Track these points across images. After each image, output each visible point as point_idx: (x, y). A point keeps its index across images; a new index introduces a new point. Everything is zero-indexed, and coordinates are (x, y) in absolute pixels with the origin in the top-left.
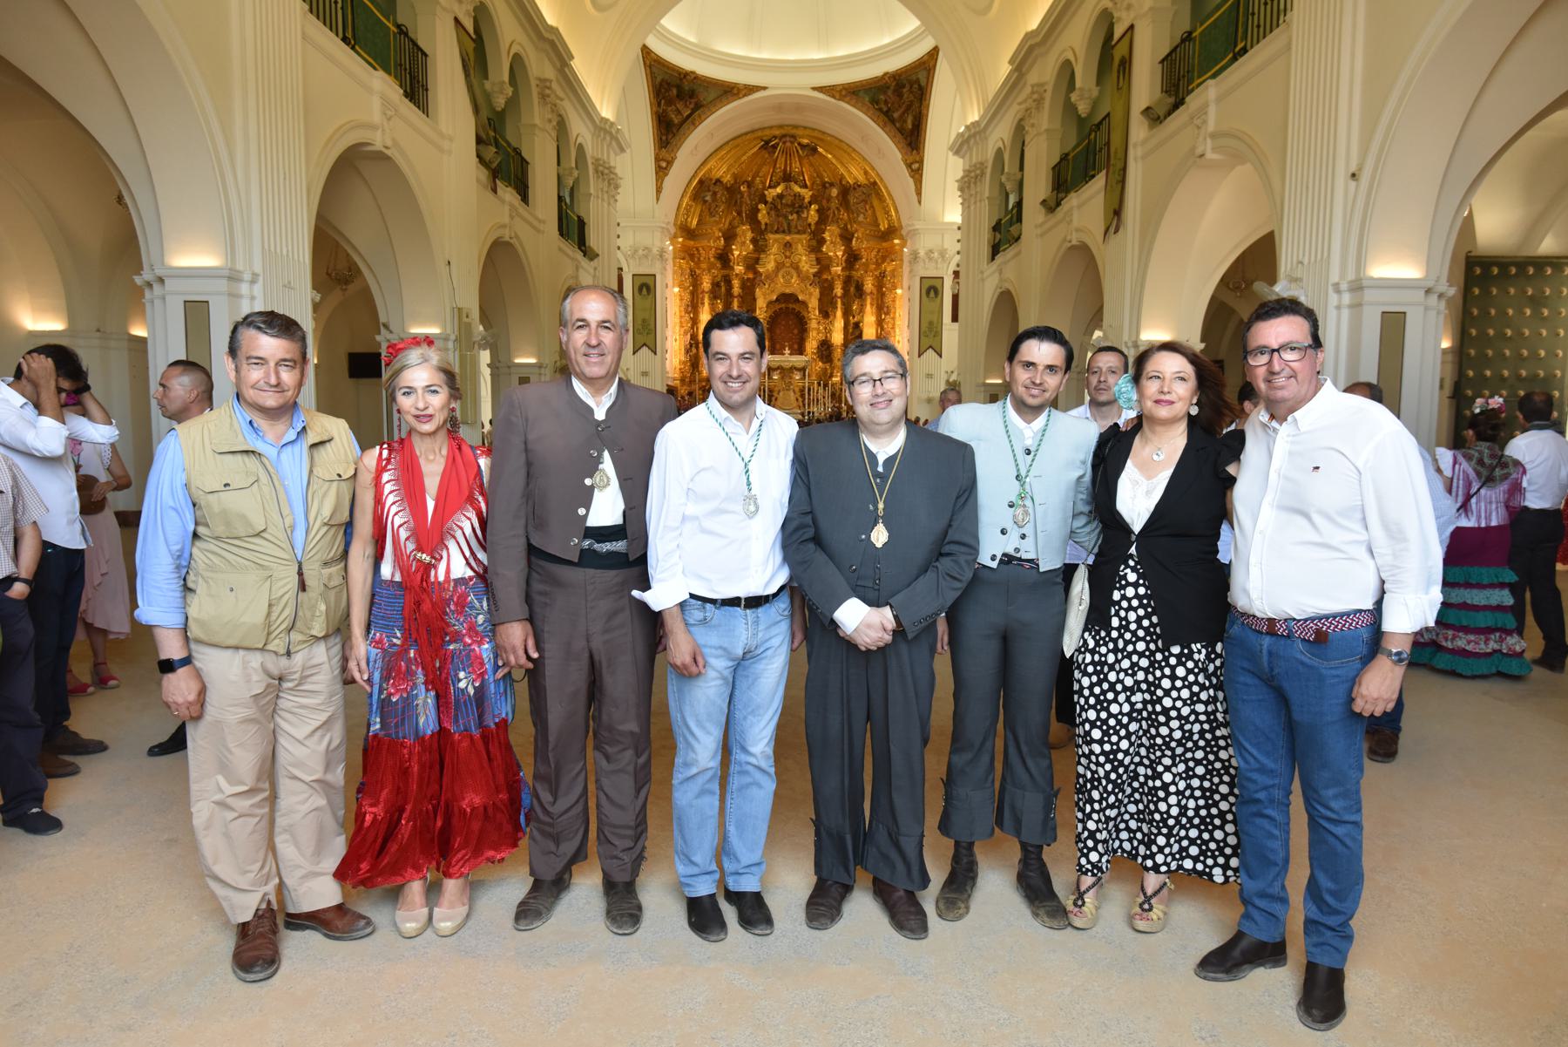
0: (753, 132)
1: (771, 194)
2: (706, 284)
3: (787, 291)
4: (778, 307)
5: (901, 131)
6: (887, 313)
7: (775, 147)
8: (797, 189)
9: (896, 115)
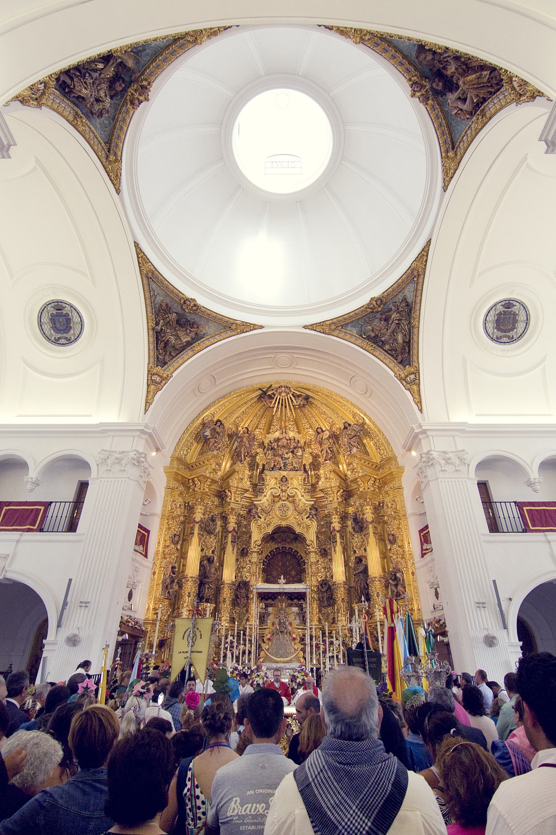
3: (284, 524)
4: (273, 546)
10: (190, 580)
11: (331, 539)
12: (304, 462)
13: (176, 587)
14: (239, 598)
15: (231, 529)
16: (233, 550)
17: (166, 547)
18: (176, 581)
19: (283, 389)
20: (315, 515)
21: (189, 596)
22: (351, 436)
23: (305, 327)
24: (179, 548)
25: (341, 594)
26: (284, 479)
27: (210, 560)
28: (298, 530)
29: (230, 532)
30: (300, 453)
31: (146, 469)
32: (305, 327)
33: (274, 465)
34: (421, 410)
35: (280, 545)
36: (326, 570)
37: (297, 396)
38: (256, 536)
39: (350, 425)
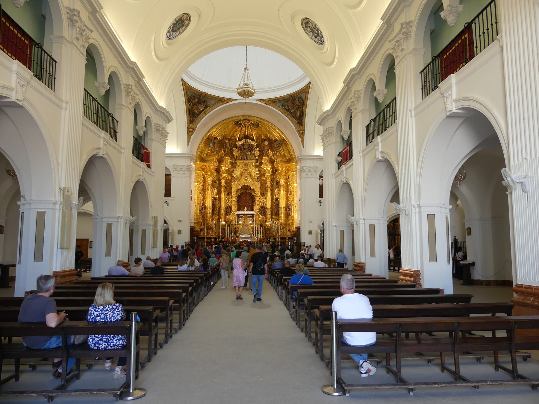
0: (231, 118)
1: (239, 143)
4: (241, 191)
5: (295, 117)
6: (290, 194)
7: (240, 124)
8: (250, 141)
9: (292, 111)
11: (266, 190)
15: (223, 186)
23: (257, 100)
25: (269, 212)
27: (215, 199)
30: (253, 153)
31: (133, 96)
32: (257, 100)
34: (303, 147)
37: (252, 124)
38: (234, 190)
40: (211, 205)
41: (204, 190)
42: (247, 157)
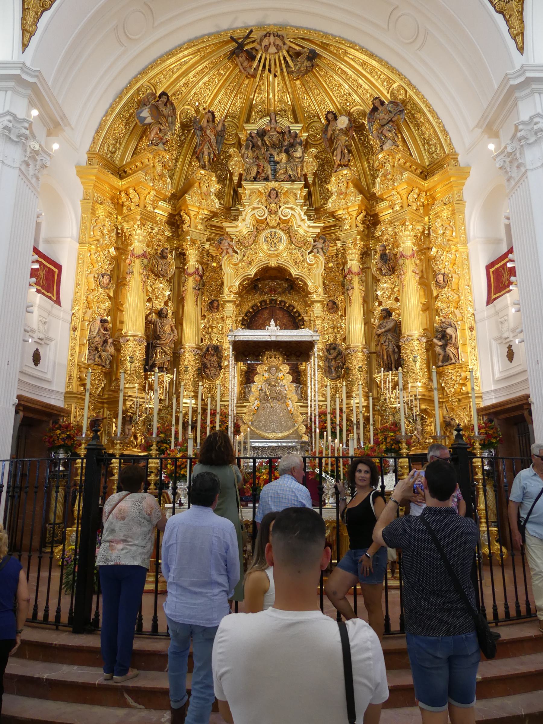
2: (138, 243)
4: (256, 299)
10: (131, 339)
11: (344, 287)
12: (305, 171)
13: (111, 350)
14: (207, 368)
15: (191, 270)
16: (197, 301)
17: (90, 291)
18: (110, 341)
19: (272, 39)
20: (322, 248)
21: (132, 362)
22: (384, 122)
24: (111, 295)
25: (357, 361)
26: (273, 195)
28: (294, 271)
29: (191, 275)
30: (298, 154)
33: (258, 173)
35: (267, 298)
36: (336, 330)
39: (382, 103)
40: (140, 331)
41: (116, 279)
42: (275, 172)
